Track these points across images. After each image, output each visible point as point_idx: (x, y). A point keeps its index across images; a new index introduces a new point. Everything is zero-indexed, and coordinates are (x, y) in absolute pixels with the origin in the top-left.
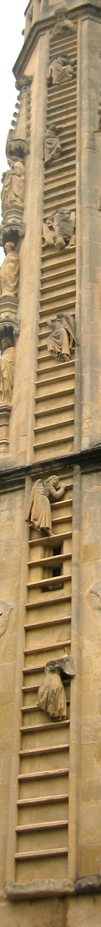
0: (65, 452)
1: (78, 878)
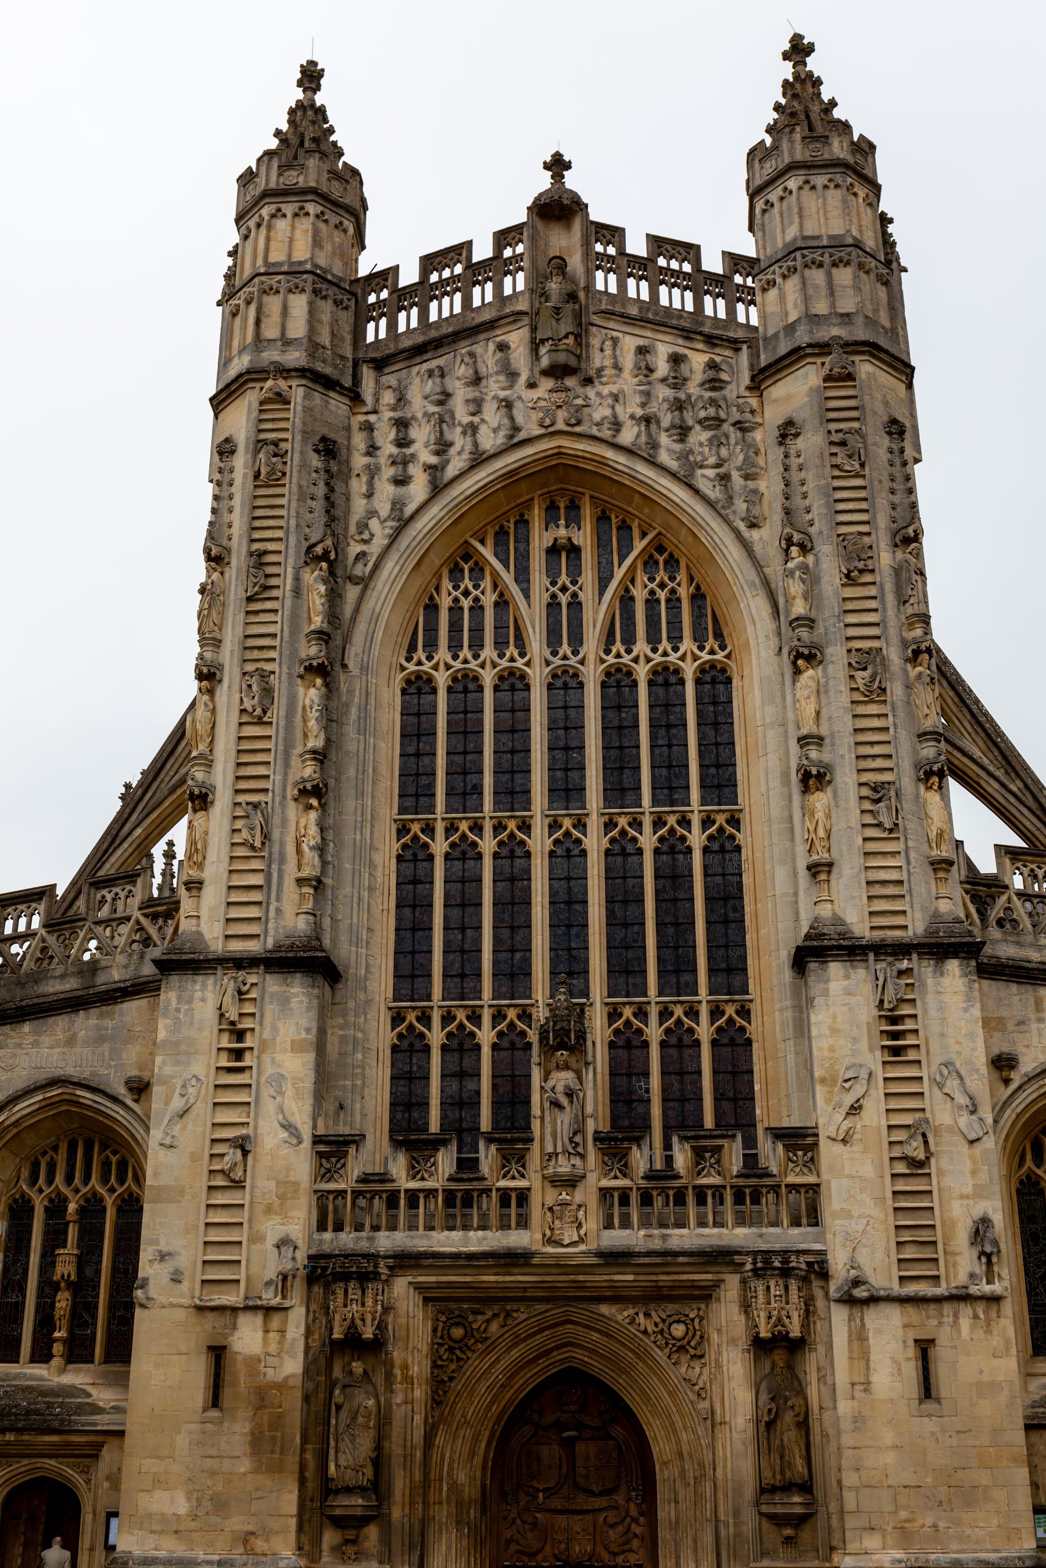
1: (246, 1298)
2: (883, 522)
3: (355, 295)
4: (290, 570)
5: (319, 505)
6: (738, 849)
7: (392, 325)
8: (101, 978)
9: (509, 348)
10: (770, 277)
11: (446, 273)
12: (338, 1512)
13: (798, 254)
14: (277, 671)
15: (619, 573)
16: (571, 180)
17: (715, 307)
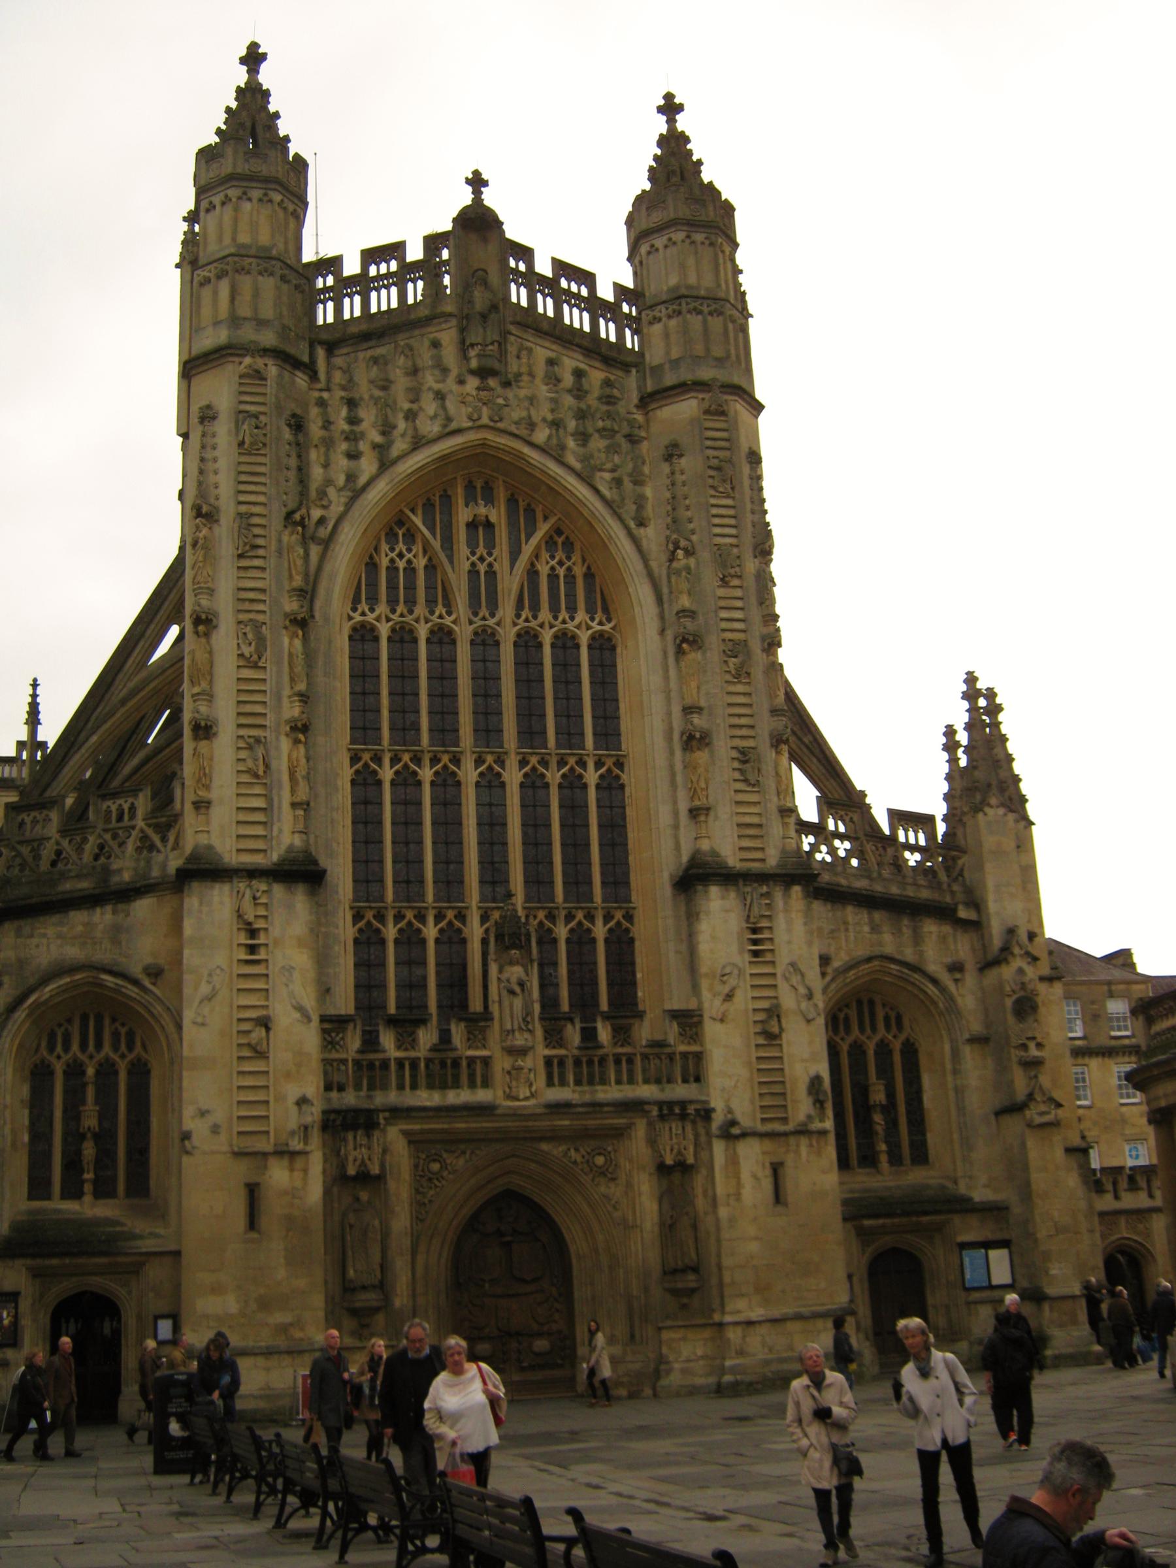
0: (258, 860)
2: (748, 539)
3: (307, 279)
4: (274, 533)
5: (292, 475)
6: (622, 787)
7: (338, 310)
8: (115, 879)
9: (441, 345)
10: (658, 314)
11: (383, 268)
12: (358, 1305)
13: (683, 301)
14: (268, 622)
15: (528, 550)
16: (490, 198)
17: (608, 331)
